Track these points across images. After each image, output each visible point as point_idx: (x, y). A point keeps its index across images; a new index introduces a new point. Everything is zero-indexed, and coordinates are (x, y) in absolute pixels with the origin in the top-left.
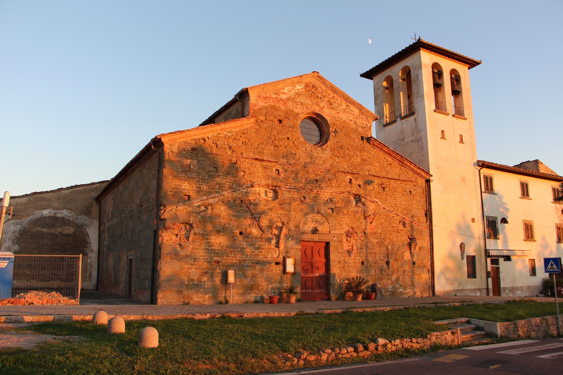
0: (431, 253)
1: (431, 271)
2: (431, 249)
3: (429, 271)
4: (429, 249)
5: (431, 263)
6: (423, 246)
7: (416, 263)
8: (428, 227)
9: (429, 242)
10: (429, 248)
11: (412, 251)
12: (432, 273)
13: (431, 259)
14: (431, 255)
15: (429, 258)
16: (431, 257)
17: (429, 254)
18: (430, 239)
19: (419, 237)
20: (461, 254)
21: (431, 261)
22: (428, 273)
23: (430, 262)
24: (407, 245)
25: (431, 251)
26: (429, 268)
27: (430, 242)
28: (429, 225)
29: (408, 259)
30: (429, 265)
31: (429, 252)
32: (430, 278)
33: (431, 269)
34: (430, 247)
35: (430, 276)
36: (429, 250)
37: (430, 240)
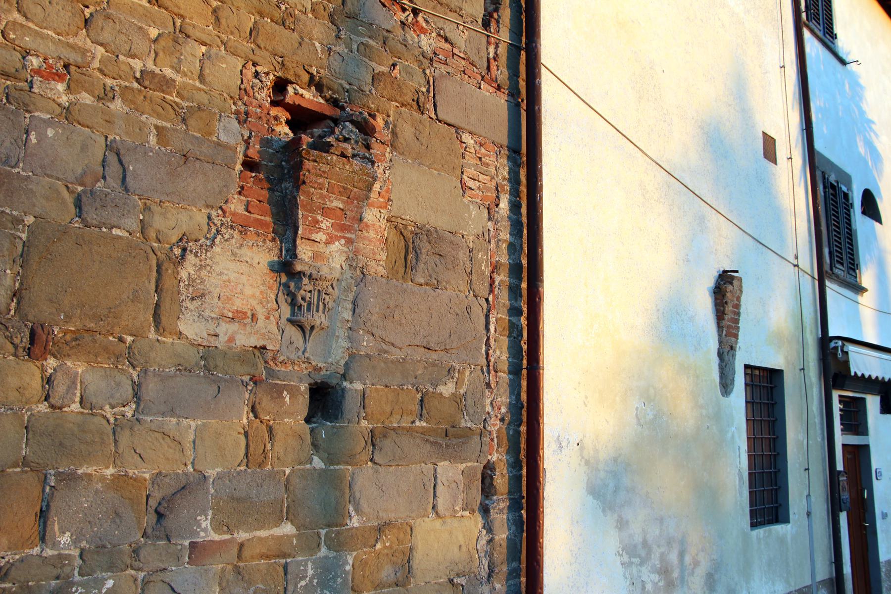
0: (515, 311)
1: (515, 480)
2: (515, 270)
3: (488, 488)
4: (495, 268)
5: (515, 407)
6: (441, 222)
7: (351, 404)
8: (501, 73)
9: (504, 204)
10: (504, 258)
11: (304, 251)
12: (515, 506)
13: (515, 371)
14: (514, 331)
15: (501, 354)
16: (515, 350)
17: (500, 315)
18: (514, 180)
19: (406, 132)
20: (720, 355)
21: (514, 387)
22: (485, 510)
23: (504, 399)
24: (249, 165)
25: (514, 291)
26: (498, 457)
27: (515, 207)
28: (514, 50)
29: (246, 339)
30: (495, 426)
31: (504, 298)
32: (501, 554)
33: (515, 465)
34: (513, 248)
35: (502, 535)
36: (502, 278)
37: (515, 193)
